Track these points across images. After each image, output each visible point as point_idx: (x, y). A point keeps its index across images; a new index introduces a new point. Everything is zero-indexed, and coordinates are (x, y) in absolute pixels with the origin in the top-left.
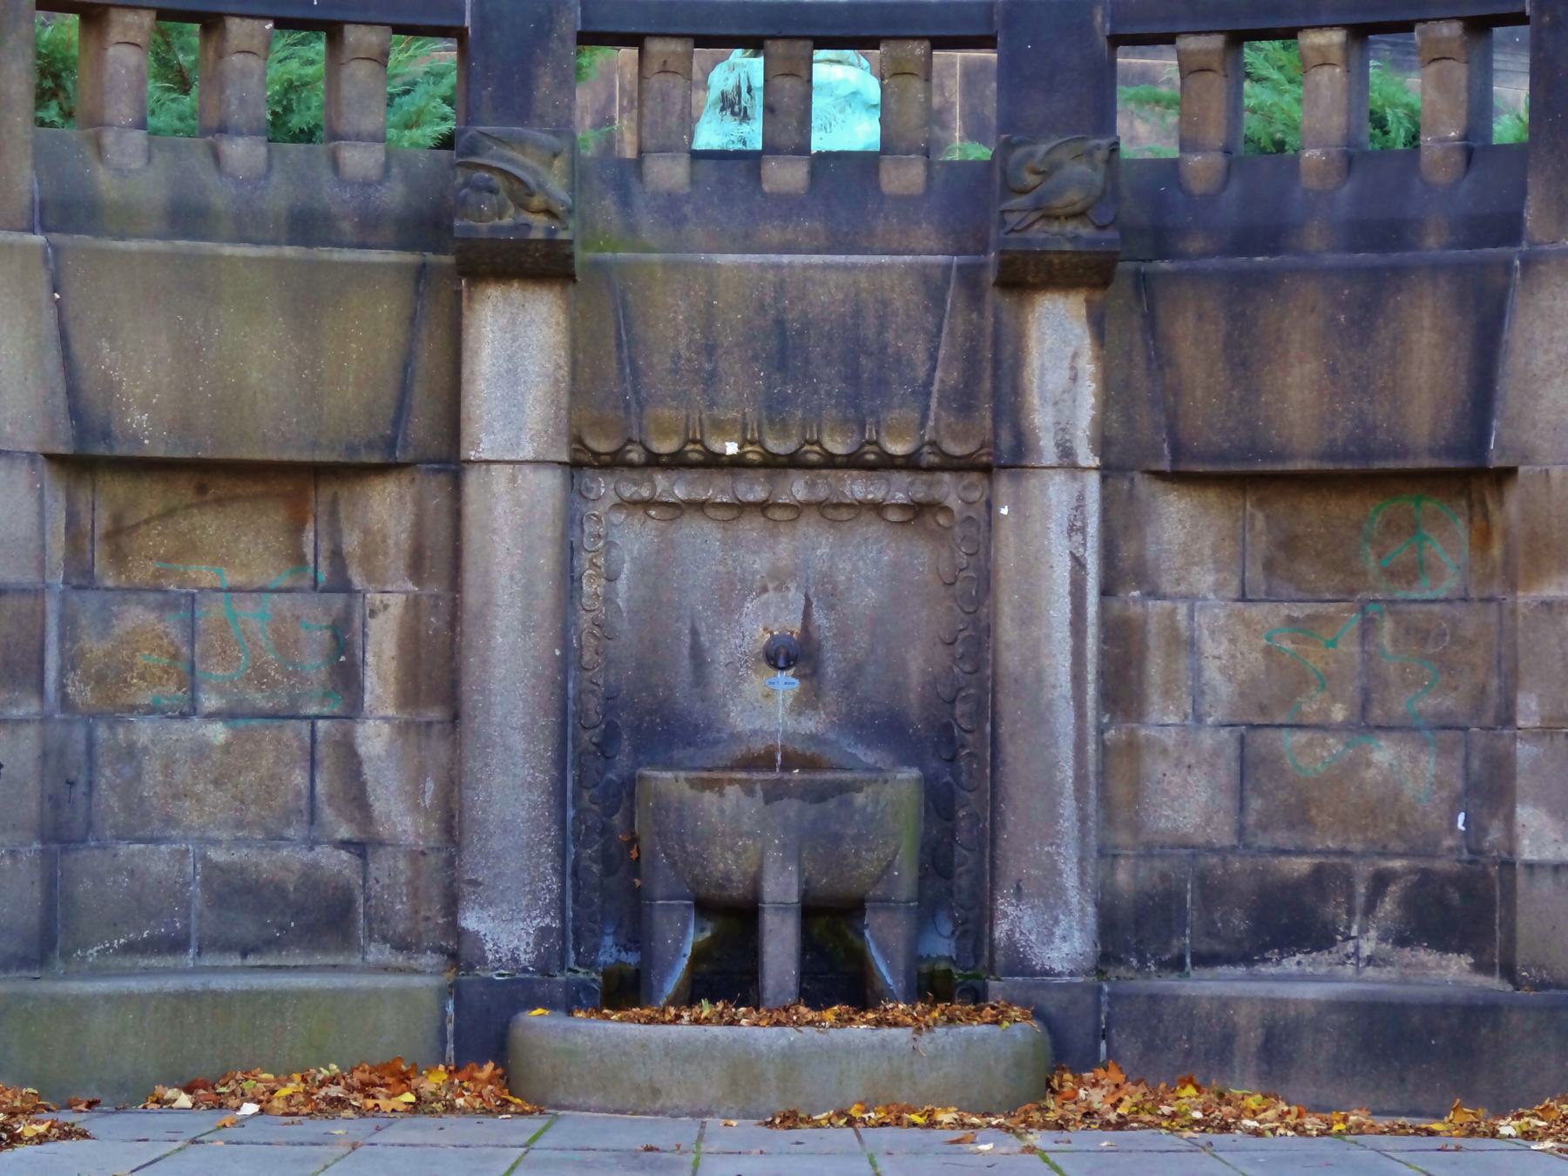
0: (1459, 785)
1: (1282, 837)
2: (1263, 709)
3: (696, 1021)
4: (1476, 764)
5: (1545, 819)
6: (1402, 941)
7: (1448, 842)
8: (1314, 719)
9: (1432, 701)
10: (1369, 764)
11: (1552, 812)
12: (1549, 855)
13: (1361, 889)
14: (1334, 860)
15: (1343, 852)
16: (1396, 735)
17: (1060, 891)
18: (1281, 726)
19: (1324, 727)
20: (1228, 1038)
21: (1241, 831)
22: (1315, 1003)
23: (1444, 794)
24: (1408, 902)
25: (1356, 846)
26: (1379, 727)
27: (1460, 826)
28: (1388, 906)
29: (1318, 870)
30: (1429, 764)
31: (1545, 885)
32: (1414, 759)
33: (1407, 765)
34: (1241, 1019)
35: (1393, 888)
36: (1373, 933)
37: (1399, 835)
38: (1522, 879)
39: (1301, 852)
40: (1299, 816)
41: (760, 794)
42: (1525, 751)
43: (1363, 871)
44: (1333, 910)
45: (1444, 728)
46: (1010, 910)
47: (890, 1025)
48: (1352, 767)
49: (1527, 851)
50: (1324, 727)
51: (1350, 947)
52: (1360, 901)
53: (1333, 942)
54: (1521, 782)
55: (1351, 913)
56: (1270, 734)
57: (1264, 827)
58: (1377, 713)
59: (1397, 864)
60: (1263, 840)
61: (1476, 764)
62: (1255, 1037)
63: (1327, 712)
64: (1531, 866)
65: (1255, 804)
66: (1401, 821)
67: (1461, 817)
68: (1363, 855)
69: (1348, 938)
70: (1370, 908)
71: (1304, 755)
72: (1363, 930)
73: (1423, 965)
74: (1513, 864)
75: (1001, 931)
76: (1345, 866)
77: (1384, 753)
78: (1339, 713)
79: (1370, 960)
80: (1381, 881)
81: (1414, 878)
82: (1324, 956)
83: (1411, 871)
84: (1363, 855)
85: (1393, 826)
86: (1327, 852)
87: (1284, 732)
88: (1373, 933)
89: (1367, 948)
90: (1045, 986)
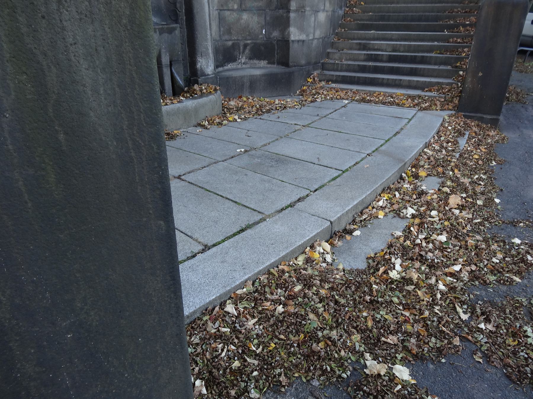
0: (263, 23)
1: (226, 37)
2: (222, 6)
3: (179, 102)
4: (268, 18)
5: (297, 30)
6: (250, 59)
7: (261, 36)
8: (231, 8)
9: (256, 4)
10: (242, 19)
11: (298, 29)
12: (297, 38)
13: (242, 48)
14: (236, 41)
15: (238, 40)
16: (248, 12)
17: (208, 54)
18: (225, 10)
19: (233, 10)
20: (243, 85)
21: (220, 36)
22: (260, 75)
23: (260, 25)
24: (252, 50)
25: (240, 38)
26: (244, 10)
27: (264, 33)
28: (247, 51)
29: (233, 44)
30: (256, 19)
31: (296, 45)
32: (252, 18)
33: (250, 19)
34: (245, 81)
35: (248, 47)
36: (244, 57)
37: (249, 35)
38: (291, 44)
39: (230, 40)
40: (229, 32)
41: (158, 32)
42: (292, 15)
43: (242, 43)
44: (236, 53)
45: (259, 10)
46: (200, 60)
47: (398, 105)
48: (239, 20)
49: (292, 38)
50: (233, 10)
51: (240, 61)
52: (241, 50)
53: (236, 60)
54: (291, 22)
55: (240, 53)
56: (223, 11)
57: (223, 34)
58: (243, 6)
59: (249, 42)
60: (224, 38)
61: (268, 18)
62: (248, 84)
63: (233, 6)
64: (293, 41)
65: (222, 29)
66: (249, 32)
67: (264, 31)
68: (242, 40)
69: (239, 59)
70: (243, 52)
71: (230, 16)
72: (242, 57)
73: (255, 63)
74: (289, 41)
75: (198, 66)
76: (239, 43)
77: (245, 16)
78: (236, 7)
79: (244, 63)
80: (245, 46)
81: (253, 45)
82: (235, 63)
83: (251, 43)
84: (242, 40)
85: (248, 33)
86: (235, 40)
87: (226, 11)
88: (244, 57)
89: (243, 61)
90: (208, 78)
